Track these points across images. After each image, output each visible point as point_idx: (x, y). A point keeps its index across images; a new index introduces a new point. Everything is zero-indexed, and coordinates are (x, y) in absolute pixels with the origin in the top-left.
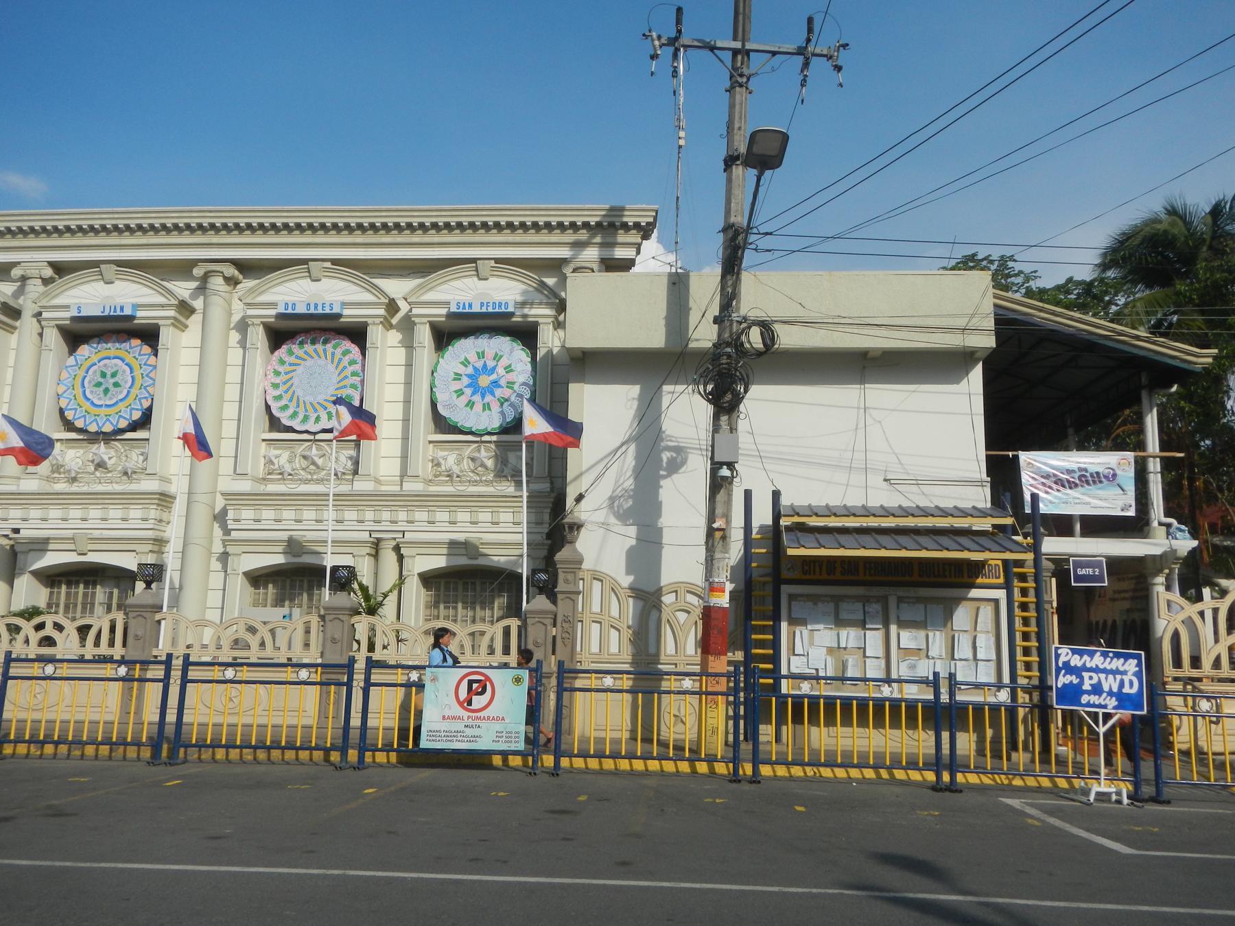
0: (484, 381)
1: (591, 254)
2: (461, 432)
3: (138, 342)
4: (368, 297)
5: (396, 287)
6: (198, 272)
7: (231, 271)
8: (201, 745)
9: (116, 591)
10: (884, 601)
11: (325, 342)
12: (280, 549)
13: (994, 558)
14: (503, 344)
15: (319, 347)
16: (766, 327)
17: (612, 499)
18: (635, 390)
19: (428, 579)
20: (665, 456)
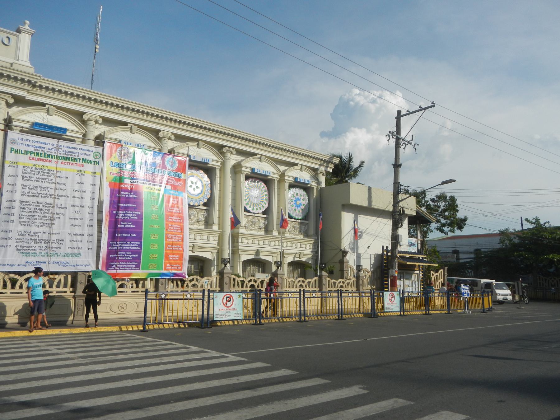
0: (298, 203)
1: (322, 169)
2: (293, 218)
3: (202, 171)
4: (275, 171)
5: (282, 168)
6: (225, 150)
7: (235, 153)
8: (310, 315)
9: (193, 266)
10: (403, 273)
11: (258, 182)
12: (254, 254)
13: (417, 264)
14: (302, 192)
15: (256, 184)
16: (403, 208)
17: (349, 244)
18: (353, 215)
19: (290, 264)
20: (359, 234)
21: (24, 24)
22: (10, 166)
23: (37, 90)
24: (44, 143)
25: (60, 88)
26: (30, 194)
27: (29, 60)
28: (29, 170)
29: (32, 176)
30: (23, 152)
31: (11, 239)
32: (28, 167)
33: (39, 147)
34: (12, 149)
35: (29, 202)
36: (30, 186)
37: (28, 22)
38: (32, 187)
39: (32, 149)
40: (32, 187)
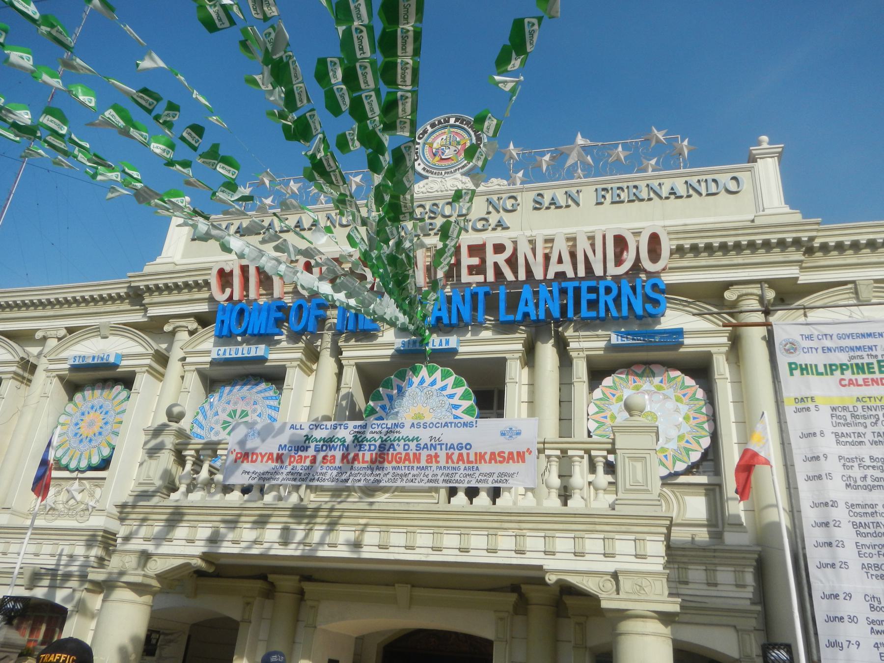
21: (759, 143)
22: (798, 410)
23: (820, 259)
24: (869, 335)
25: (871, 237)
26: (869, 481)
27: (786, 203)
28: (848, 415)
29: (861, 429)
30: (821, 369)
31: (853, 619)
32: (845, 409)
33: (859, 348)
34: (792, 367)
35: (872, 506)
36: (862, 460)
37: (765, 138)
38: (868, 462)
39: (842, 358)
40: (868, 462)
